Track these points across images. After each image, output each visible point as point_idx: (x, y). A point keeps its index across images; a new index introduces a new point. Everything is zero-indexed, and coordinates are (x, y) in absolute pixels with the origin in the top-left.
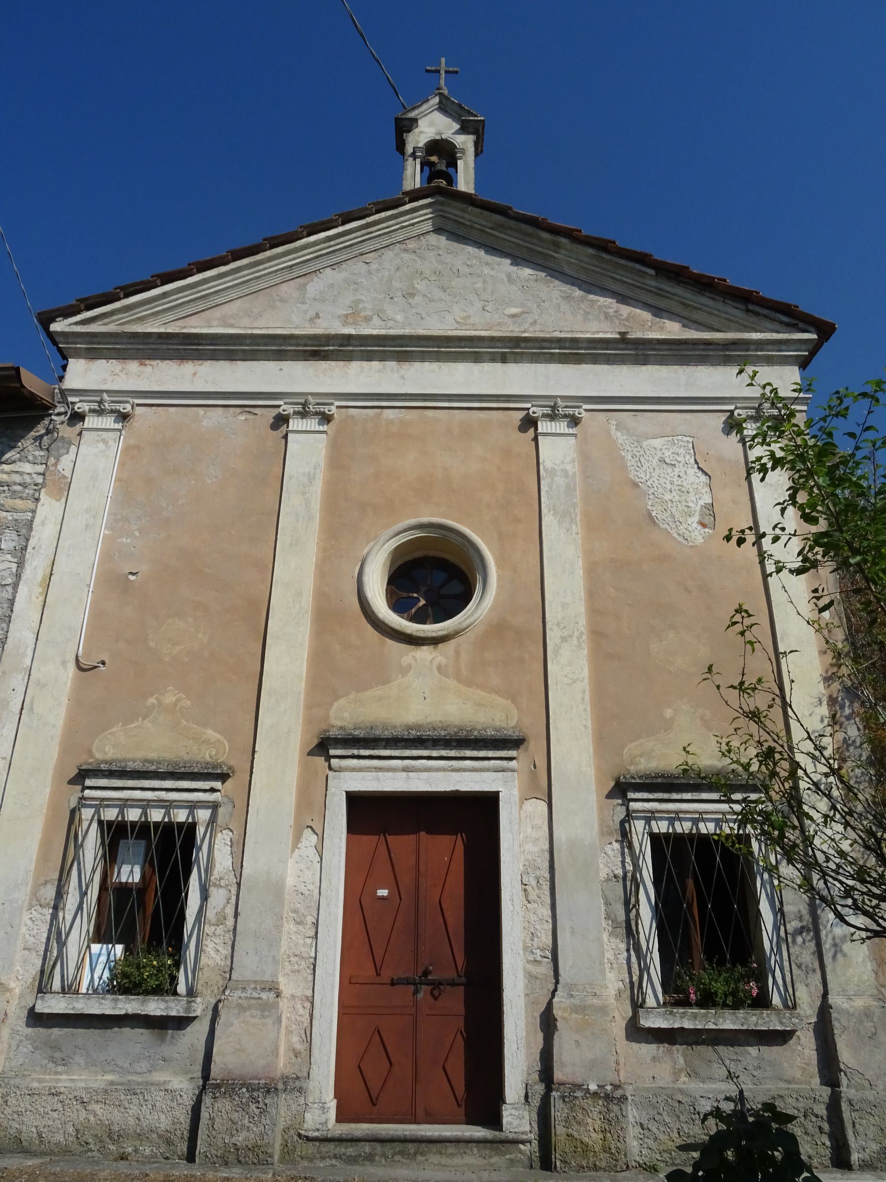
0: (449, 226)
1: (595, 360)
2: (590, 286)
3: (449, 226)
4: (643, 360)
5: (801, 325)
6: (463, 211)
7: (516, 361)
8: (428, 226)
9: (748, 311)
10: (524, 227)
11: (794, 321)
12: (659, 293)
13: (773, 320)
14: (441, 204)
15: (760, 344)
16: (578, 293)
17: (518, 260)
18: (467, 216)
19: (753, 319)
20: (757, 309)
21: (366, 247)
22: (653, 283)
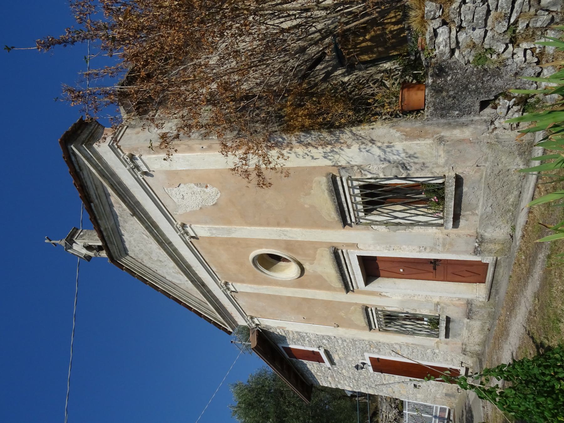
0: (123, 252)
1: (149, 218)
2: (114, 216)
3: (123, 252)
4: (138, 203)
5: (71, 151)
6: (114, 252)
7: (168, 239)
8: (127, 257)
9: (81, 170)
10: (106, 238)
11: (71, 155)
12: (99, 197)
13: (77, 161)
14: (117, 258)
15: (96, 167)
16: (119, 218)
17: (121, 235)
18: (116, 251)
19: (83, 167)
20: (77, 168)
21: (151, 272)
22: (96, 201)
